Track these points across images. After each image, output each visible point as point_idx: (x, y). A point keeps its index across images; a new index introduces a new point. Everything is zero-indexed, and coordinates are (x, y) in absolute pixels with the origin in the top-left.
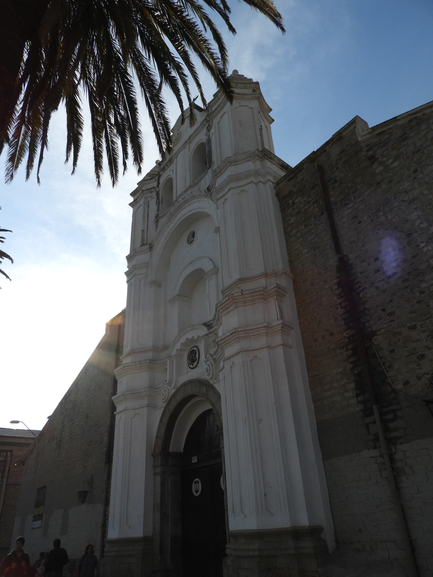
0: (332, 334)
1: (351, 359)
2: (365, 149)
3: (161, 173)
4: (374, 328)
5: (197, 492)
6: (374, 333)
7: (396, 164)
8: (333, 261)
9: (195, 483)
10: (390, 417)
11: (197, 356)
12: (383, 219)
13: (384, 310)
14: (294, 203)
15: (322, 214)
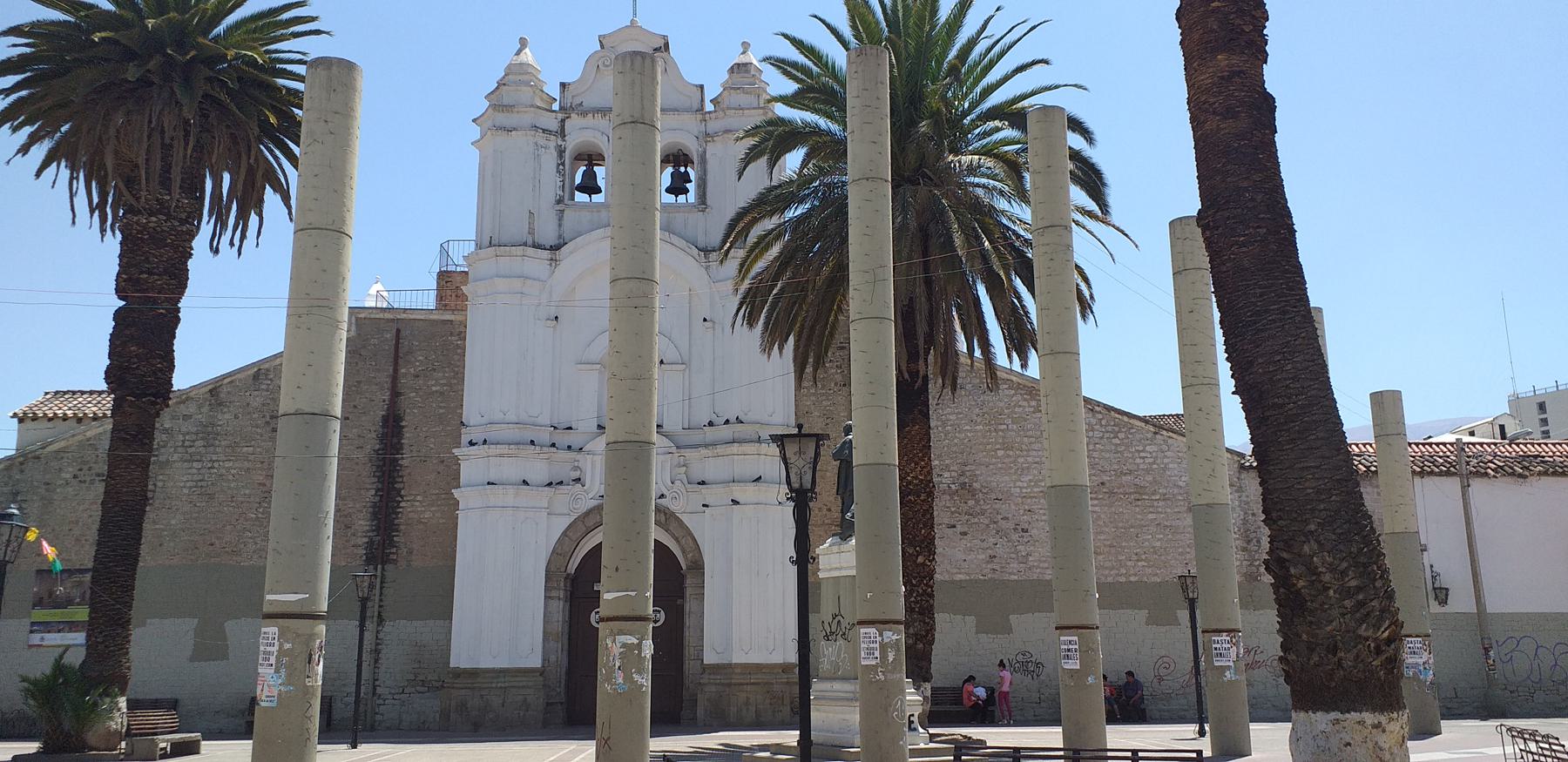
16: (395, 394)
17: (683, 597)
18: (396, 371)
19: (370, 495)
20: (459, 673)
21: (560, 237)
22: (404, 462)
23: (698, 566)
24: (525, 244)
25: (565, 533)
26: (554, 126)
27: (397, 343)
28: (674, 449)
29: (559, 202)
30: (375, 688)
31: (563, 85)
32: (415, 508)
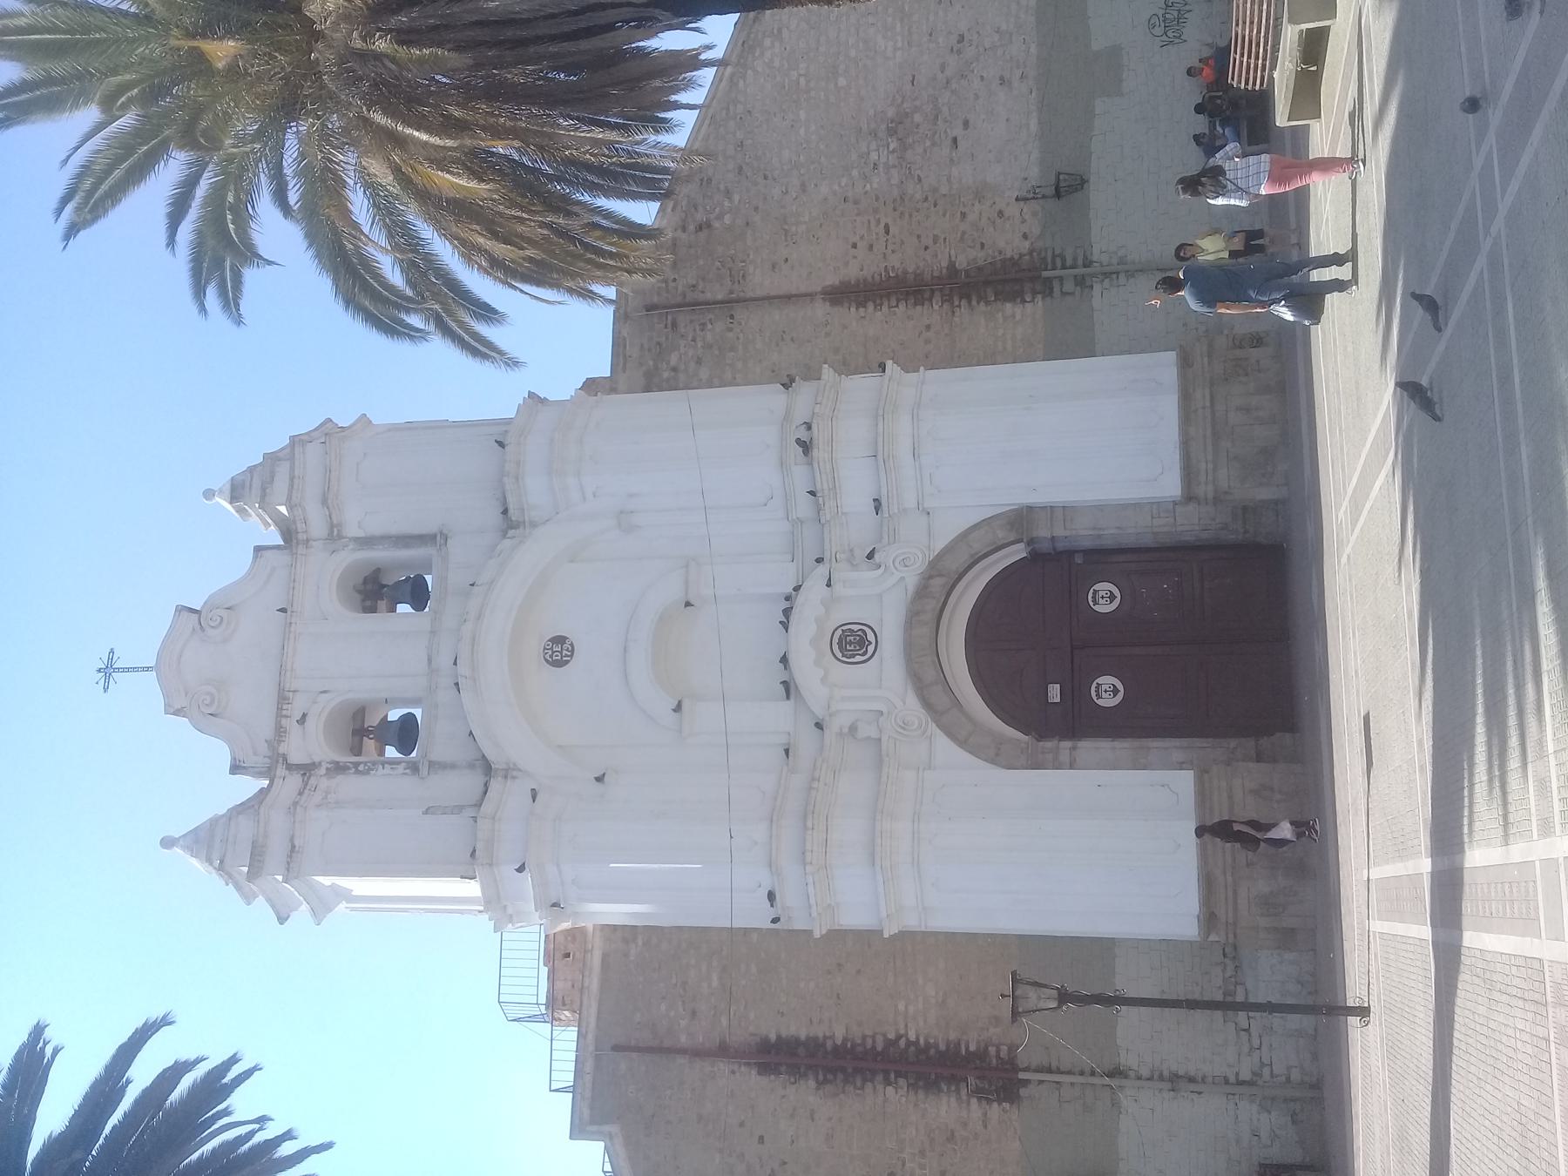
0: (928, 327)
1: (974, 303)
2: (679, 233)
3: (281, 750)
4: (945, 264)
5: (1115, 691)
6: (952, 265)
7: (736, 198)
8: (820, 309)
9: (1099, 697)
10: (1059, 263)
11: (855, 627)
12: (804, 227)
13: (926, 248)
14: (674, 369)
15: (732, 317)
16: (723, 1051)
17: (1071, 553)
18: (683, 1051)
19: (895, 1096)
20: (1209, 919)
21: (471, 766)
22: (839, 1034)
23: (1021, 519)
24: (475, 819)
25: (962, 743)
26: (295, 780)
27: (638, 1049)
28: (822, 570)
29: (414, 768)
30: (1240, 1083)
31: (236, 768)
32: (919, 1014)
